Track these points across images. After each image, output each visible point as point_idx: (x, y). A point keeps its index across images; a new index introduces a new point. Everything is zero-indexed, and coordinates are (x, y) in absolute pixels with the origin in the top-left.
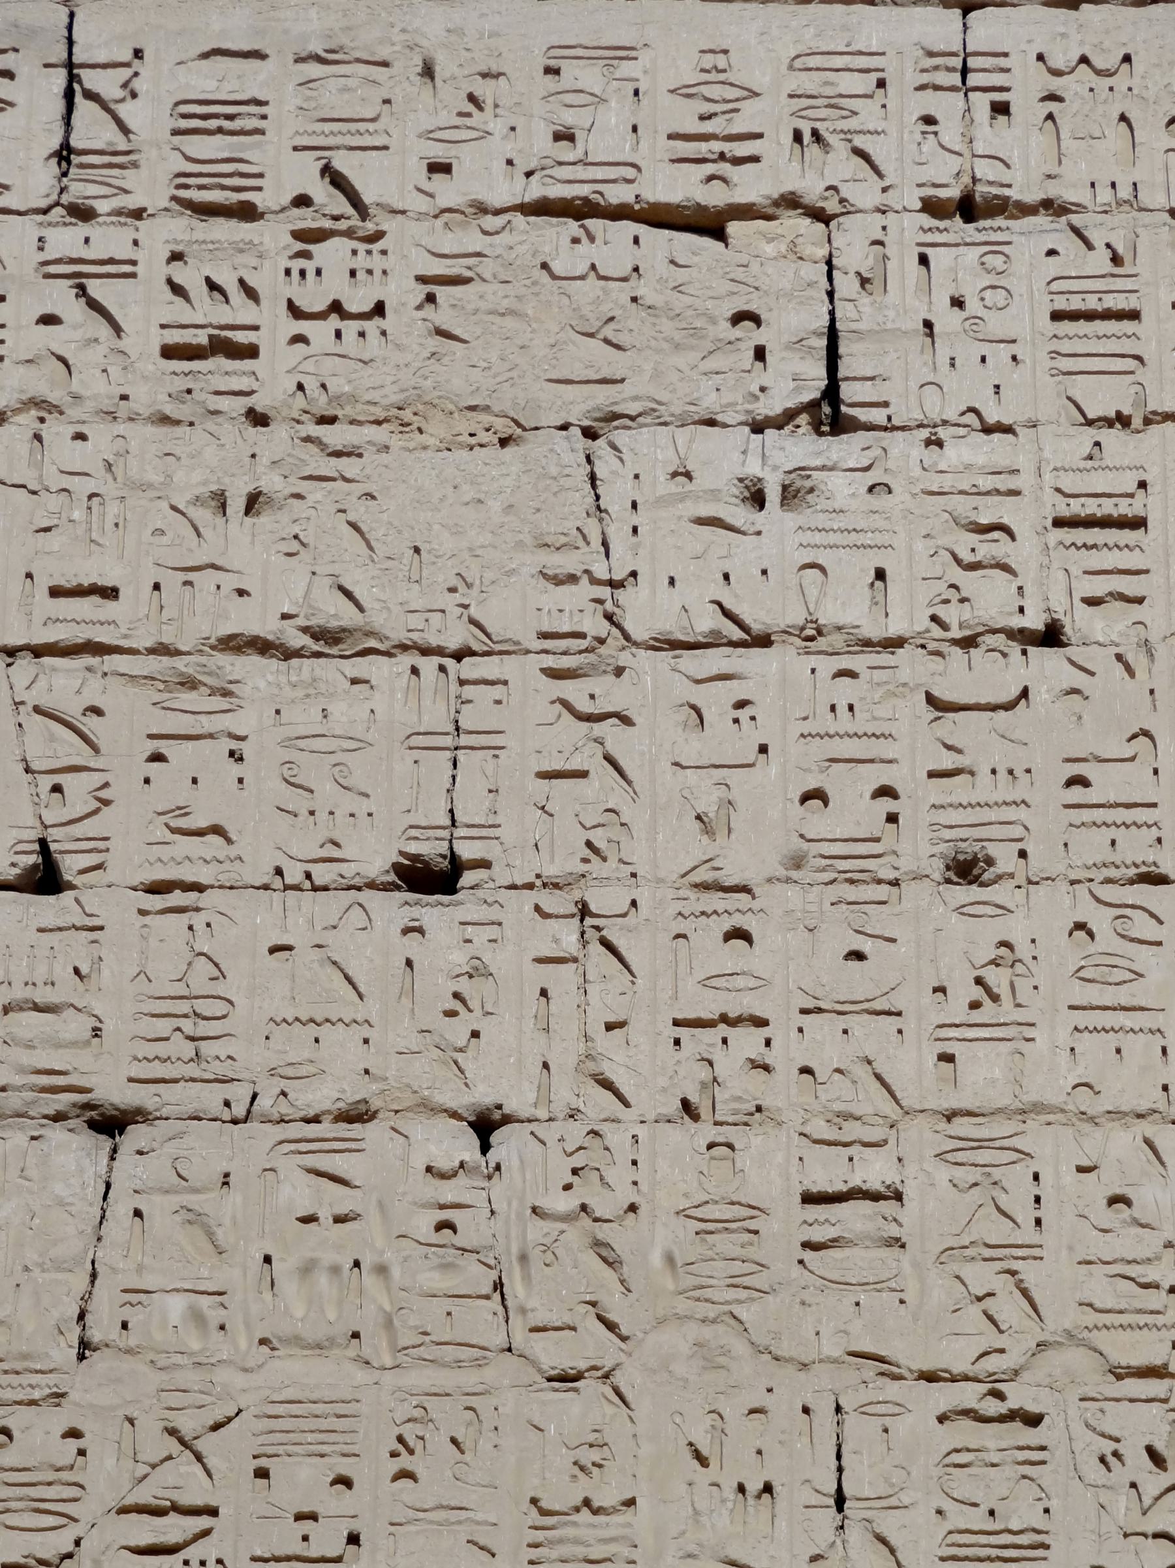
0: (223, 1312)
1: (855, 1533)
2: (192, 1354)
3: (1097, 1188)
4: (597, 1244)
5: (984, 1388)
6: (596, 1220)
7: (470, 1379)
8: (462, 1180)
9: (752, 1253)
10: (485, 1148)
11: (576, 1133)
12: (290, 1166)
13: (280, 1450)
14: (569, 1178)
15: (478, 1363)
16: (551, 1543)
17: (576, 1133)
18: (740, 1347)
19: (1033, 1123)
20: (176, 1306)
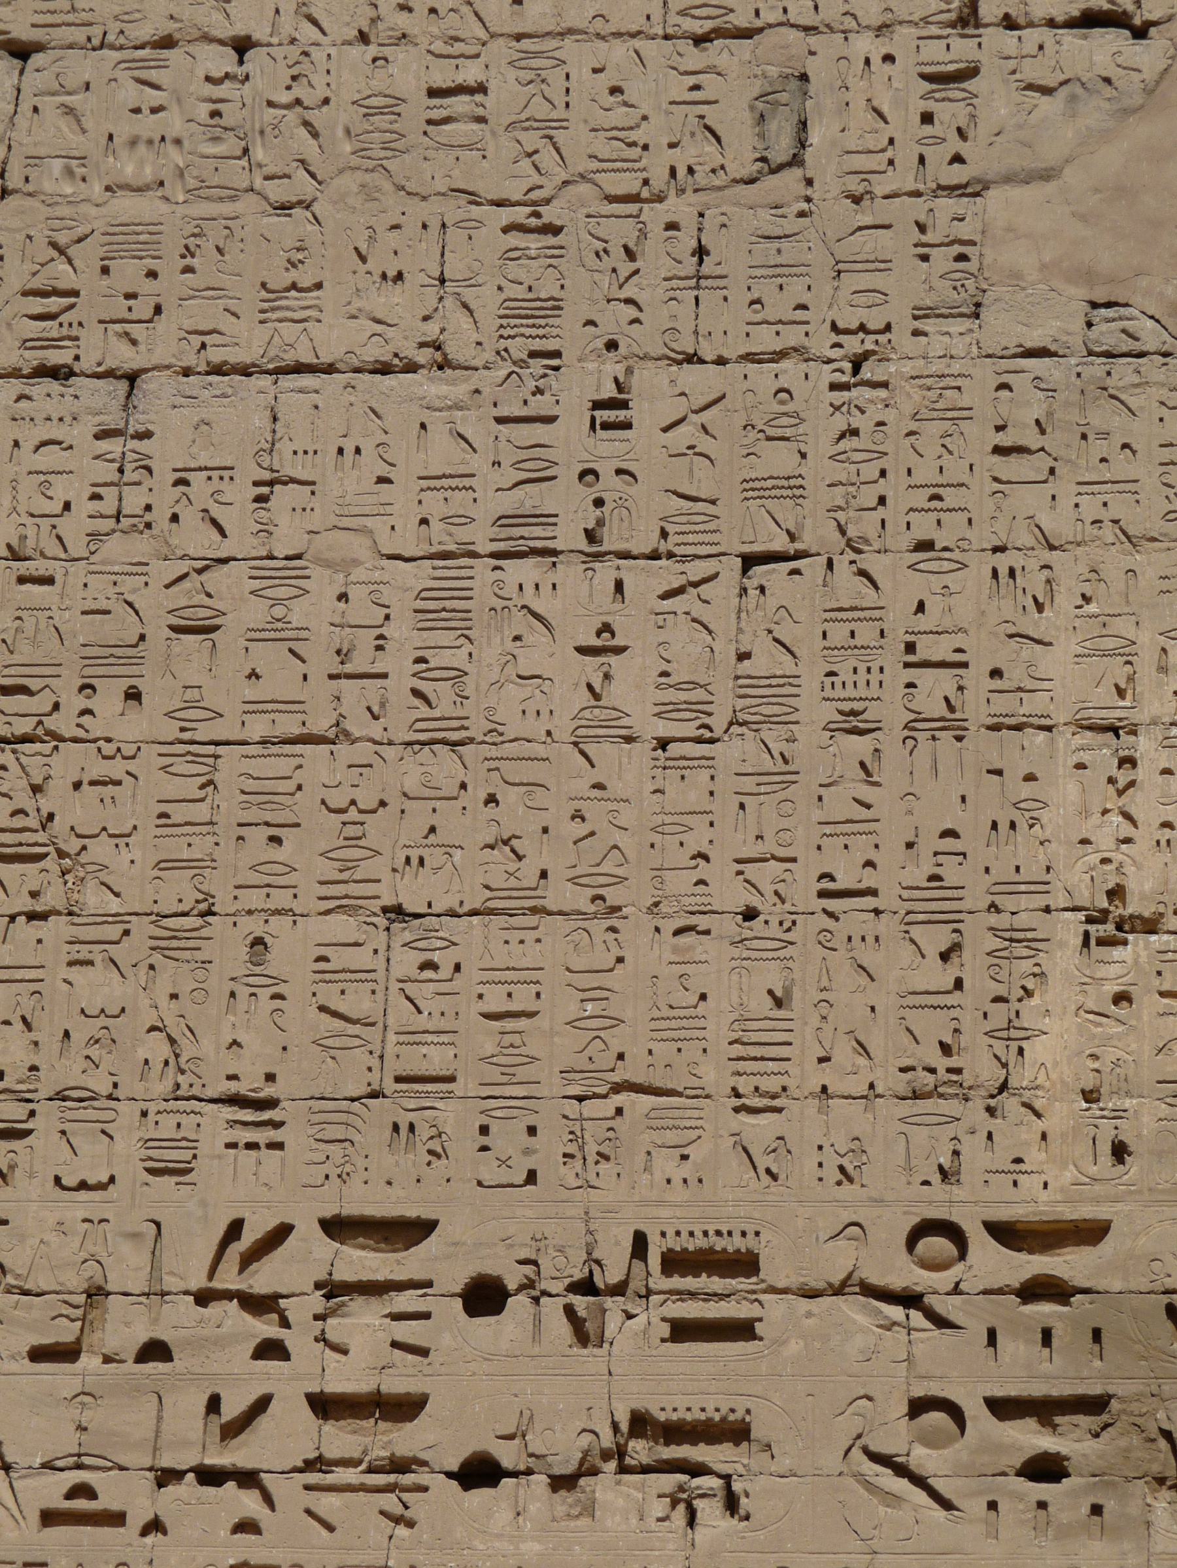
0: (84, 170)
1: (449, 302)
2: (66, 196)
3: (605, 81)
4: (306, 124)
5: (528, 210)
6: (306, 108)
7: (227, 208)
8: (227, 84)
9: (395, 126)
10: (241, 62)
11: (294, 52)
12: (124, 76)
13: (116, 254)
14: (289, 82)
15: (233, 198)
16: (273, 309)
17: (294, 52)
18: (387, 186)
19: (568, 41)
20: (58, 164)
